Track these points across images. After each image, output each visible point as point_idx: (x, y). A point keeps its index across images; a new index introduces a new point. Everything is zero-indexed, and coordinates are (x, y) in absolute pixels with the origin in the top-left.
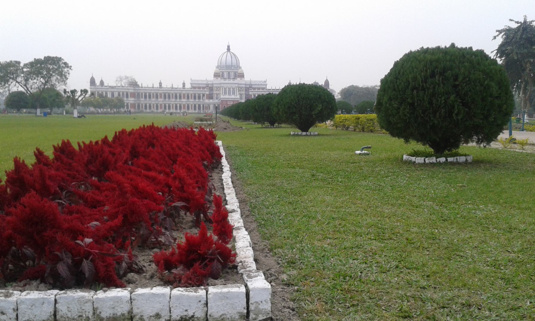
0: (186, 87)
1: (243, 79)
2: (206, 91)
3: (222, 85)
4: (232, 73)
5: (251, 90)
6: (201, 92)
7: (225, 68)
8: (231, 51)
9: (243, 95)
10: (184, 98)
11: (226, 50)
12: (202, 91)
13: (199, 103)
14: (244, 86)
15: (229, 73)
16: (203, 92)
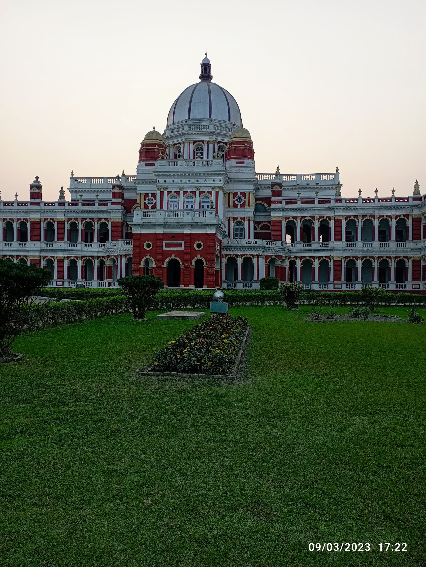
0: (45, 198)
1: (246, 161)
2: (109, 212)
3: (161, 183)
4: (211, 145)
5: (280, 202)
6: (96, 216)
7: (186, 129)
8: (212, 81)
9: (247, 222)
10: (36, 237)
11: (199, 81)
12: (99, 212)
13: (88, 255)
14: (249, 188)
15: (200, 148)
16: (103, 216)
